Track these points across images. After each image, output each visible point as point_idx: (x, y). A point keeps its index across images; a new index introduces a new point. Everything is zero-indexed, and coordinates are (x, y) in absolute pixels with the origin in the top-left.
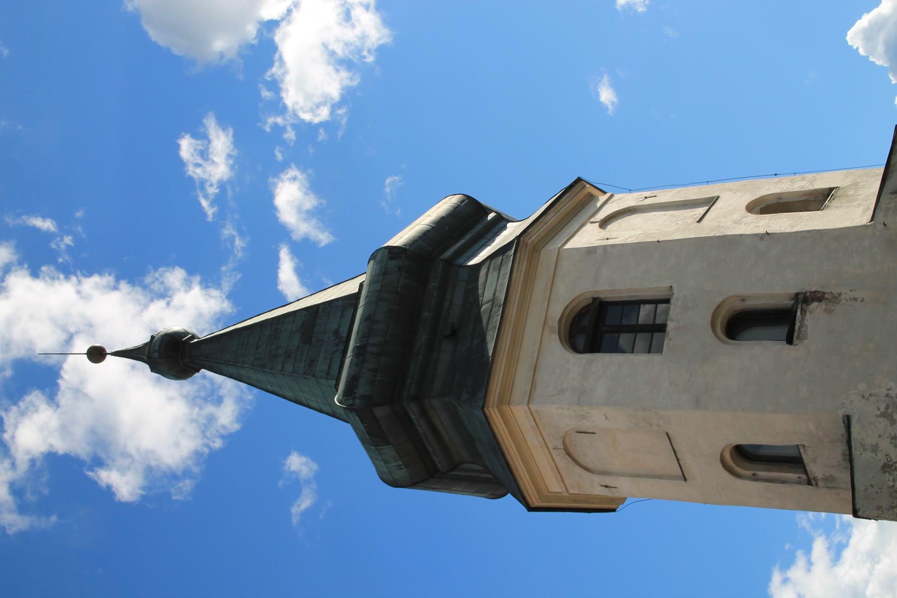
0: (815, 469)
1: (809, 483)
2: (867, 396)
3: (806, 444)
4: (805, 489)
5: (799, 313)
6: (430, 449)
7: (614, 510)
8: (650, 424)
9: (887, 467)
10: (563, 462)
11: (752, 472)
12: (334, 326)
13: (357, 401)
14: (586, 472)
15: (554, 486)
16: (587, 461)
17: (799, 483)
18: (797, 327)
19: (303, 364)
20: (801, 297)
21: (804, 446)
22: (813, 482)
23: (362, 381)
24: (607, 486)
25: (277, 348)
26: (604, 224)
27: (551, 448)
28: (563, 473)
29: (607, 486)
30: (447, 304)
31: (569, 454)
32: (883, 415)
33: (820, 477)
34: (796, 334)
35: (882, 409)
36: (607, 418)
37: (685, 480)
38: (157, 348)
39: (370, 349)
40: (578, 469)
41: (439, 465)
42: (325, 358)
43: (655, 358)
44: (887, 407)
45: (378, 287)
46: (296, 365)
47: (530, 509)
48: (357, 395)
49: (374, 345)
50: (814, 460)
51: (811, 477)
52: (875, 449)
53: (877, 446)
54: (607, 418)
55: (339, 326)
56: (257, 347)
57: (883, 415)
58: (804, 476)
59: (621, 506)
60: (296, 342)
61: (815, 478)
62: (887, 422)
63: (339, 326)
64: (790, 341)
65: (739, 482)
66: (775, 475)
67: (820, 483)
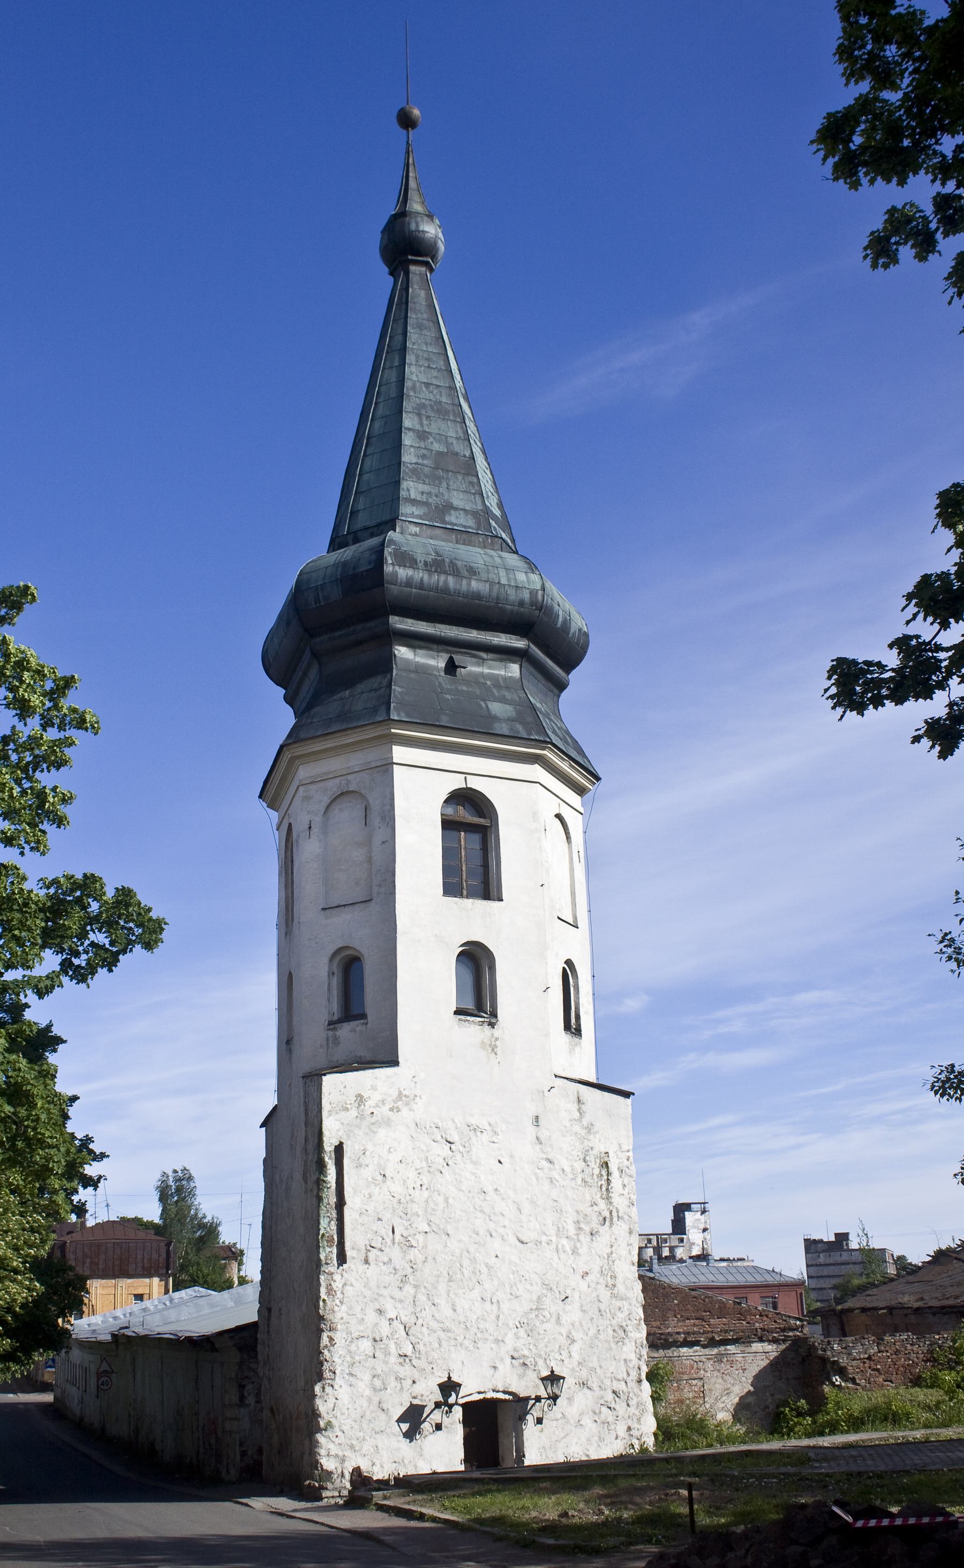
0: (345, 1031)
1: (330, 1023)
2: (415, 1080)
3: (369, 1025)
4: (324, 1018)
5: (482, 1019)
6: (338, 633)
7: (260, 797)
8: (380, 885)
9: (360, 1099)
10: (333, 786)
11: (335, 971)
12: (456, 502)
13: (391, 568)
14: (323, 809)
15: (304, 772)
16: (335, 811)
17: (329, 1014)
18: (469, 1018)
19: (414, 460)
20: (493, 1021)
21: (366, 1024)
22: (331, 1027)
23: (410, 572)
24: (310, 828)
25: (428, 417)
26: (558, 816)
27: (349, 777)
28: (321, 784)
29: (310, 828)
30: (484, 655)
31: (342, 794)
32: (400, 1093)
33: (339, 1033)
34: (462, 1017)
35: (404, 1093)
36: (383, 842)
37: (324, 909)
38: (421, 229)
39: (443, 578)
40: (326, 800)
41: (318, 639)
42: (422, 493)
43: (441, 890)
44: (406, 1096)
45: (504, 581)
46: (412, 450)
47: (282, 747)
48: (397, 568)
49: (446, 582)
50: (353, 1031)
51: (337, 1026)
52: (374, 1088)
53: (376, 1089)
54: (383, 842)
55: (456, 509)
56: (427, 385)
57: (400, 1093)
58: (336, 1018)
59: (265, 805)
60: (437, 447)
61: (335, 1029)
62: (394, 1097)
63: (456, 509)
64: (458, 1012)
65: (326, 960)
66: (335, 992)
67: (331, 1033)
